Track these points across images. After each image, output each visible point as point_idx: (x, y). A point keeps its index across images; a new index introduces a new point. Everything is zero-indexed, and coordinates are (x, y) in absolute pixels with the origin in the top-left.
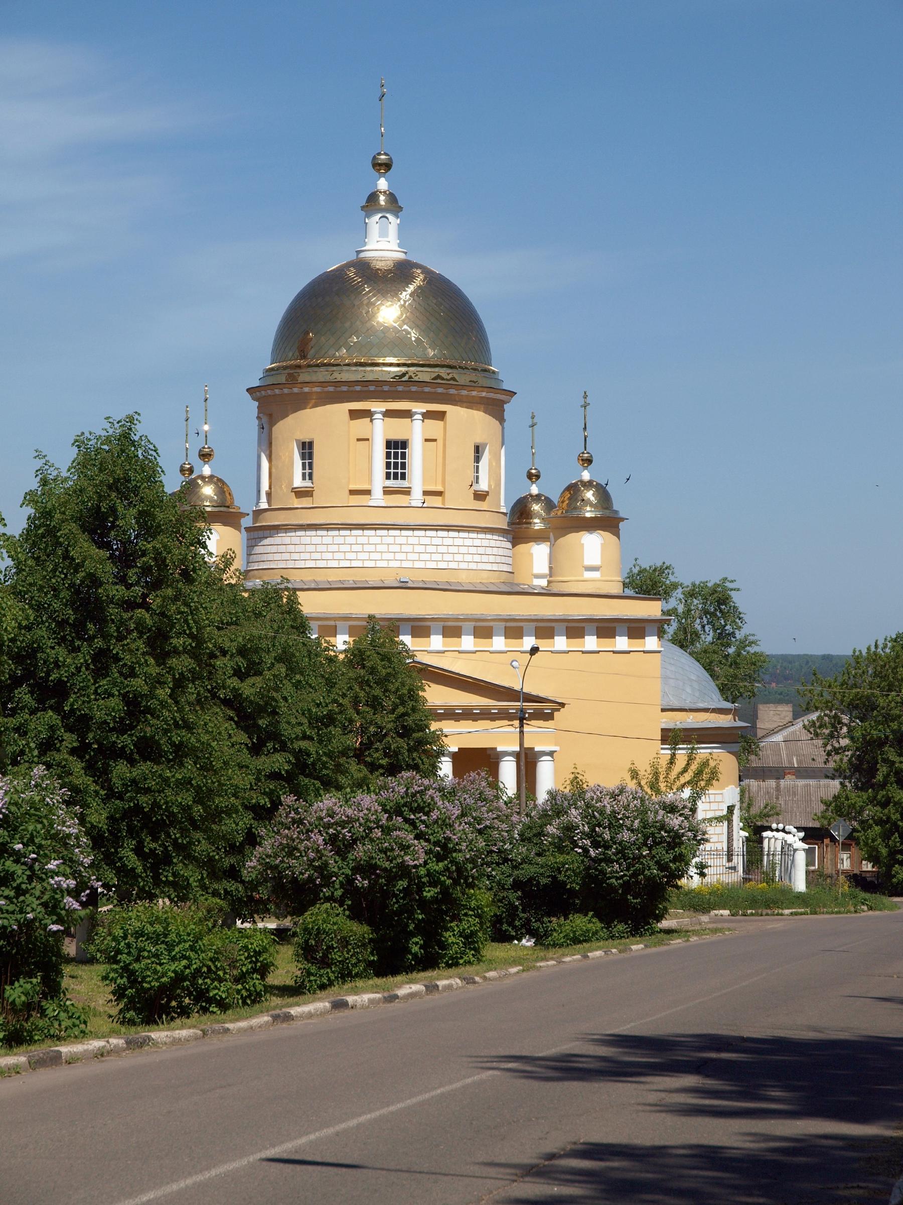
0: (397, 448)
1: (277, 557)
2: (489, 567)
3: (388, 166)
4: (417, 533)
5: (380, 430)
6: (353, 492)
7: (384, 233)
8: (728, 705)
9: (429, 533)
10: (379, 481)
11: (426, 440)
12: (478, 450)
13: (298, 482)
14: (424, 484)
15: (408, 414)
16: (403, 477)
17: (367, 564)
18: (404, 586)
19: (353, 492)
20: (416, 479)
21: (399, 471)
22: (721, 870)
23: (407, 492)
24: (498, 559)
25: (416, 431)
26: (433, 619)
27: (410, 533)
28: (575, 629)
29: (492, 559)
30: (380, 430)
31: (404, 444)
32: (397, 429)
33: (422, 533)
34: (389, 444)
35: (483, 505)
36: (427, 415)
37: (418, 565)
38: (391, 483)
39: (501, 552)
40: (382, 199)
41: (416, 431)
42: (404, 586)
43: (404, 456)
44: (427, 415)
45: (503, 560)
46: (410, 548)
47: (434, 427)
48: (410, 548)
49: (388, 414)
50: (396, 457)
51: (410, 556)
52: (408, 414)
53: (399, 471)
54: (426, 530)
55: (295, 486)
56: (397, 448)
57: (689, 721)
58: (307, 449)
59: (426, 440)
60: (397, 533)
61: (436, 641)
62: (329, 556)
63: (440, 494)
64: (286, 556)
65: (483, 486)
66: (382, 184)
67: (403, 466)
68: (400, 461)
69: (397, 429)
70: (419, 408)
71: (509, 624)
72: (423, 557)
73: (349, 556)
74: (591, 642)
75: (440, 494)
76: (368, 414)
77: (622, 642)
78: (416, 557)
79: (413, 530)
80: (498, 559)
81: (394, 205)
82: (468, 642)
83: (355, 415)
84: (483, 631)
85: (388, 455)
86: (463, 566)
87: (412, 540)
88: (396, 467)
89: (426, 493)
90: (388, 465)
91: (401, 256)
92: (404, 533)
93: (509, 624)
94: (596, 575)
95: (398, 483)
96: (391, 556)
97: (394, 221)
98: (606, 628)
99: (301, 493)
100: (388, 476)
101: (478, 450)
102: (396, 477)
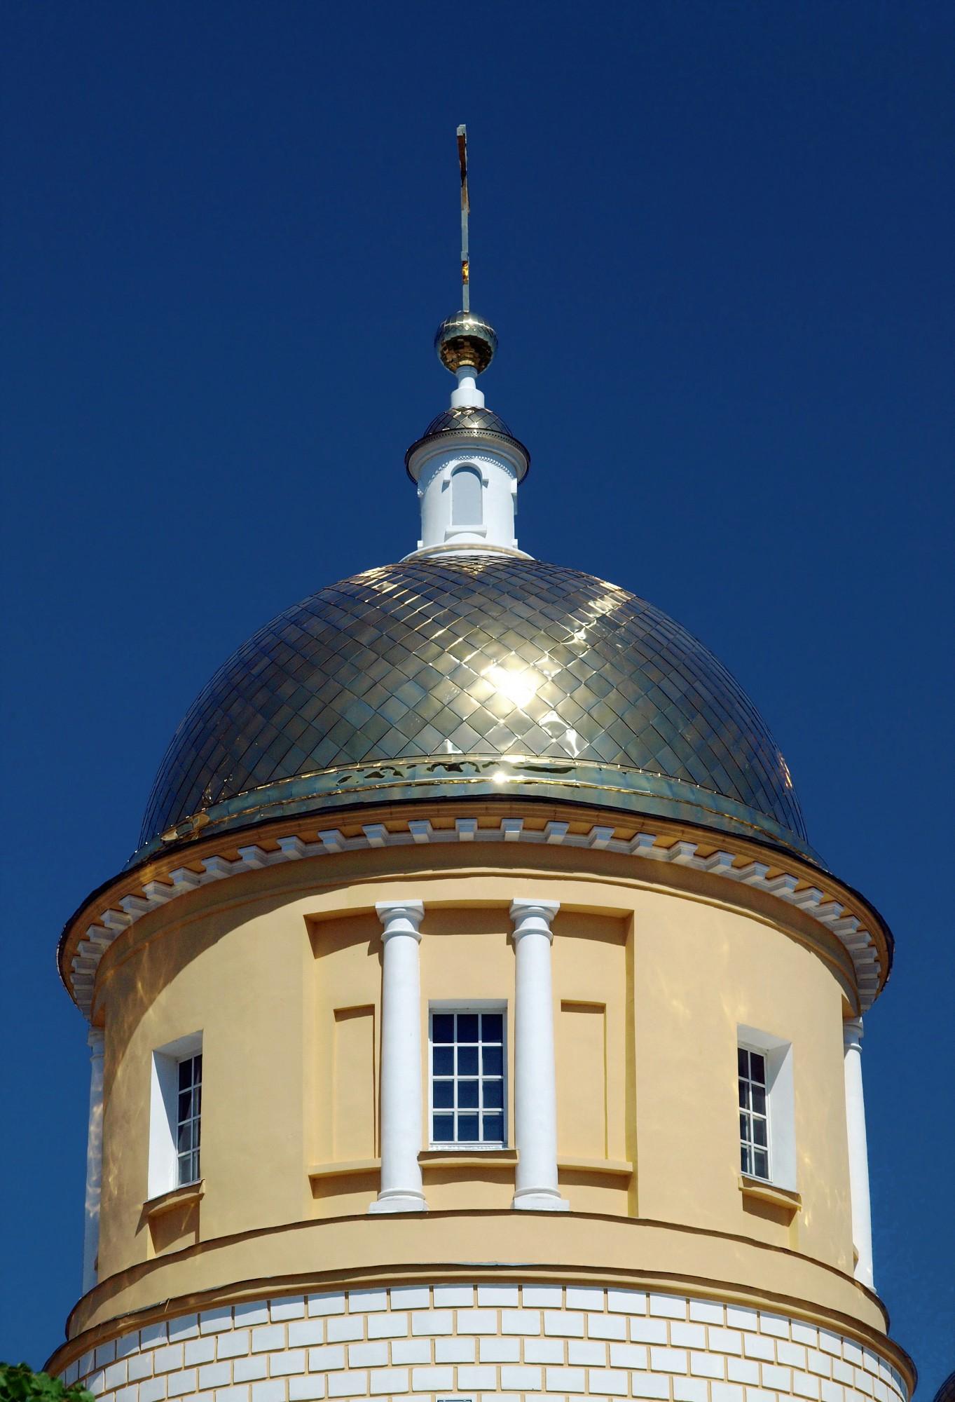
0: (470, 1037)
4: (534, 1295)
5: (416, 975)
6: (323, 1184)
9: (576, 1297)
11: (567, 1006)
21: (482, 1111)
23: (508, 1175)
27: (507, 1295)
30: (416, 975)
31: (494, 1024)
32: (469, 970)
33: (551, 1295)
34: (441, 1025)
43: (496, 1061)
46: (509, 1349)
47: (595, 962)
48: (509, 1349)
50: (468, 1060)
53: (482, 1111)
54: (565, 1284)
55: (153, 1193)
56: (470, 1037)
59: (567, 1006)
67: (496, 1094)
68: (481, 1077)
69: (469, 970)
79: (520, 1283)
85: (442, 1061)
87: (514, 1321)
89: (568, 1175)
90: (442, 1094)
92: (489, 1294)
100: (442, 1128)
102: (468, 1128)
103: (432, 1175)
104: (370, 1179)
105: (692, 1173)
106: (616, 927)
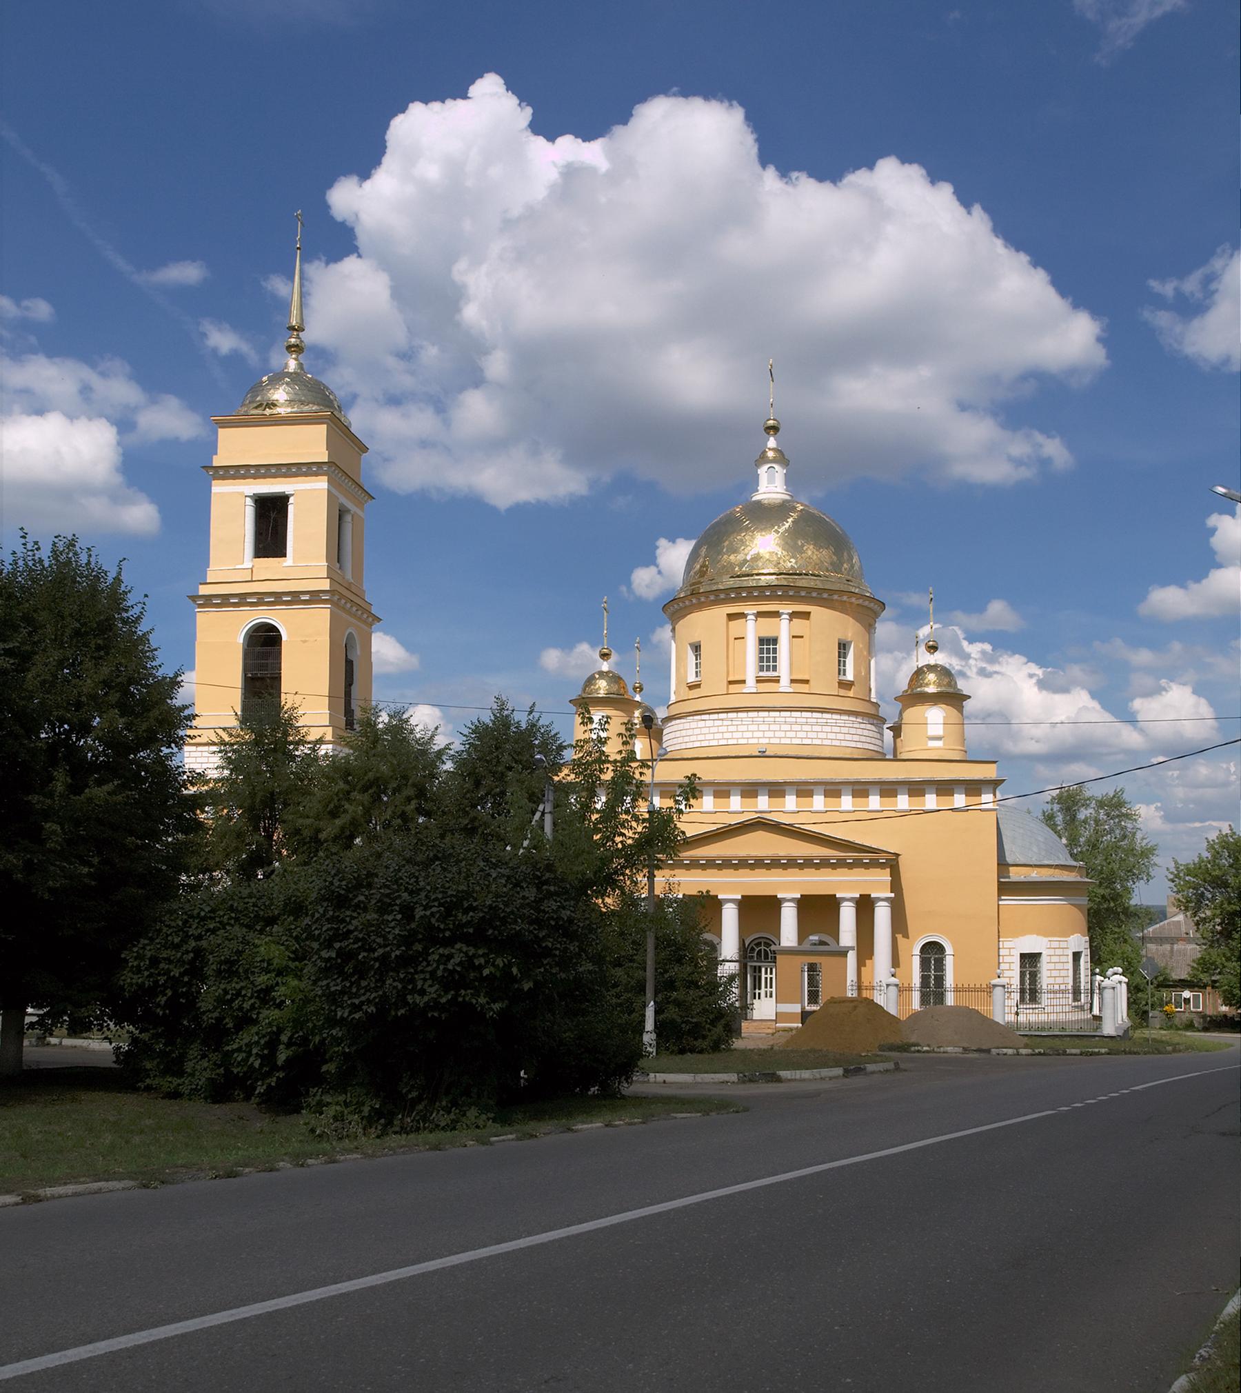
0: (768, 644)
1: (675, 741)
2: (853, 745)
3: (774, 429)
4: (783, 714)
5: (751, 630)
6: (730, 683)
7: (771, 480)
8: (1074, 863)
10: (751, 671)
12: (843, 647)
13: (692, 678)
14: (791, 673)
15: (776, 614)
16: (775, 668)
17: (741, 741)
18: (763, 755)
19: (730, 683)
20: (784, 671)
22: (1067, 1009)
23: (777, 680)
24: (863, 739)
25: (783, 629)
26: (785, 783)
28: (916, 788)
29: (856, 738)
30: (751, 630)
31: (775, 641)
32: (767, 627)
34: (762, 641)
35: (851, 694)
36: (794, 615)
37: (783, 741)
38: (764, 674)
39: (871, 734)
40: (770, 454)
41: (783, 629)
42: (763, 755)
43: (775, 651)
44: (794, 615)
45: (868, 740)
49: (760, 615)
51: (777, 734)
52: (776, 614)
56: (768, 644)
57: (1034, 875)
58: (697, 648)
60: (766, 714)
61: (791, 802)
62: (711, 736)
63: (807, 682)
64: (680, 740)
65: (850, 676)
66: (772, 442)
67: (775, 659)
70: (786, 608)
71: (856, 787)
72: (789, 734)
73: (726, 735)
74: (931, 801)
75: (807, 682)
76: (743, 616)
77: (960, 800)
78: (783, 734)
80: (863, 739)
81: (781, 458)
82: (819, 802)
83: (731, 617)
84: (833, 790)
85: (761, 651)
86: (829, 742)
88: (768, 659)
89: (793, 681)
91: (788, 498)
92: (772, 714)
93: (856, 787)
94: (939, 744)
95: (771, 674)
96: (760, 734)
97: (780, 471)
98: (945, 788)
99: (692, 687)
101: (843, 647)
103: (759, 681)
104: (744, 682)
105: (825, 682)
106: (806, 615)
